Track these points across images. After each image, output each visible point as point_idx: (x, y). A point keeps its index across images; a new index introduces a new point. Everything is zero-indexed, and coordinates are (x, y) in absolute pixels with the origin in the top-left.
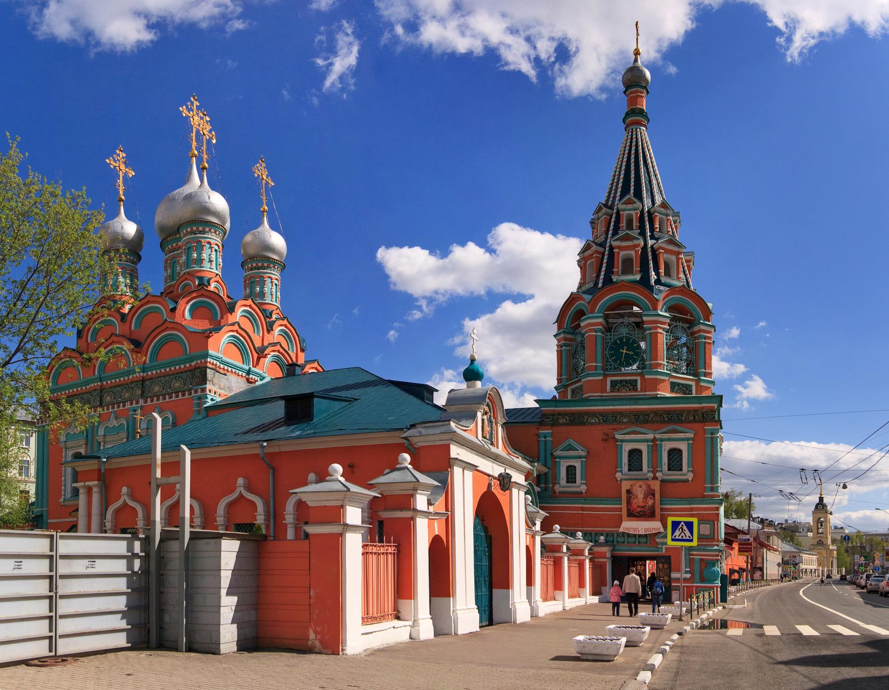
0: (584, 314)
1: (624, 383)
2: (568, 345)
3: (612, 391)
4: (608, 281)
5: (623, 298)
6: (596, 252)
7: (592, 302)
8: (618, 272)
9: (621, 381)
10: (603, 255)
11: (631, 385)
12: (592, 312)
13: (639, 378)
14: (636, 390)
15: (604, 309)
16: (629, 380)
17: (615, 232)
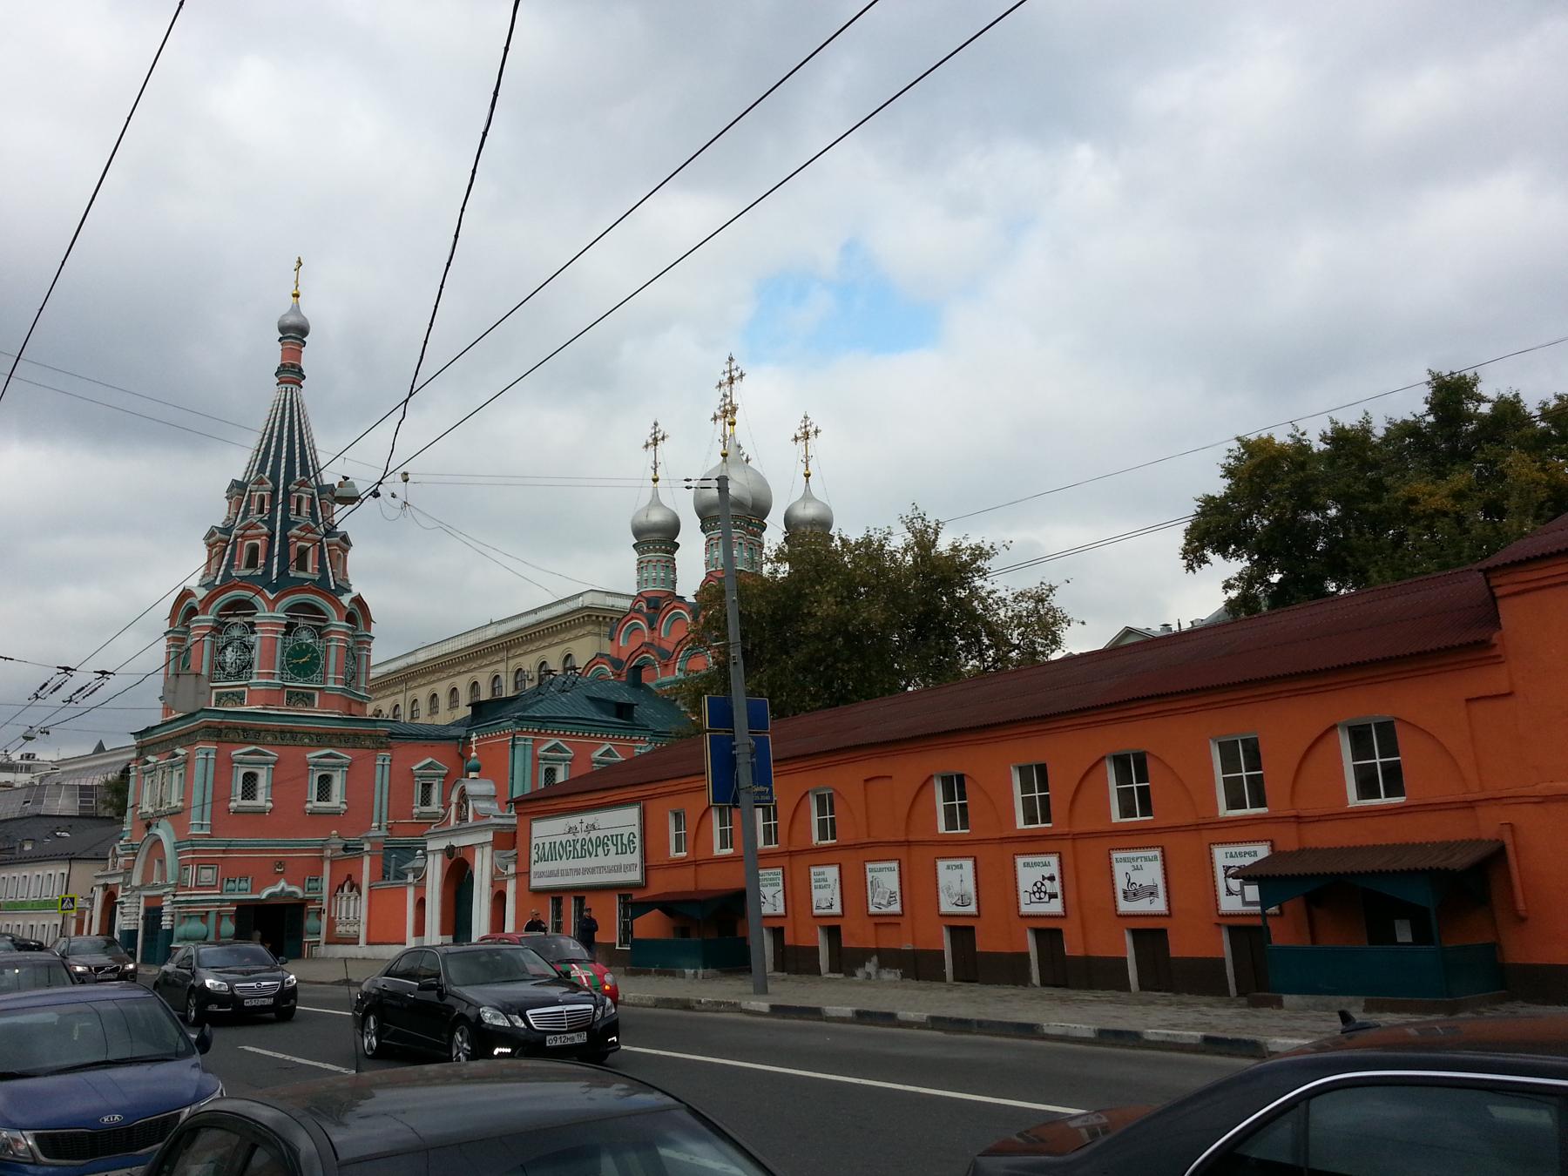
0: (197, 614)
1: (230, 696)
2: (178, 647)
3: (216, 706)
4: (227, 575)
5: (238, 598)
6: (221, 541)
7: (204, 601)
8: (239, 566)
9: (227, 694)
10: (227, 542)
11: (238, 698)
12: (205, 611)
13: (246, 689)
14: (242, 705)
15: (219, 607)
16: (237, 692)
17: (244, 517)
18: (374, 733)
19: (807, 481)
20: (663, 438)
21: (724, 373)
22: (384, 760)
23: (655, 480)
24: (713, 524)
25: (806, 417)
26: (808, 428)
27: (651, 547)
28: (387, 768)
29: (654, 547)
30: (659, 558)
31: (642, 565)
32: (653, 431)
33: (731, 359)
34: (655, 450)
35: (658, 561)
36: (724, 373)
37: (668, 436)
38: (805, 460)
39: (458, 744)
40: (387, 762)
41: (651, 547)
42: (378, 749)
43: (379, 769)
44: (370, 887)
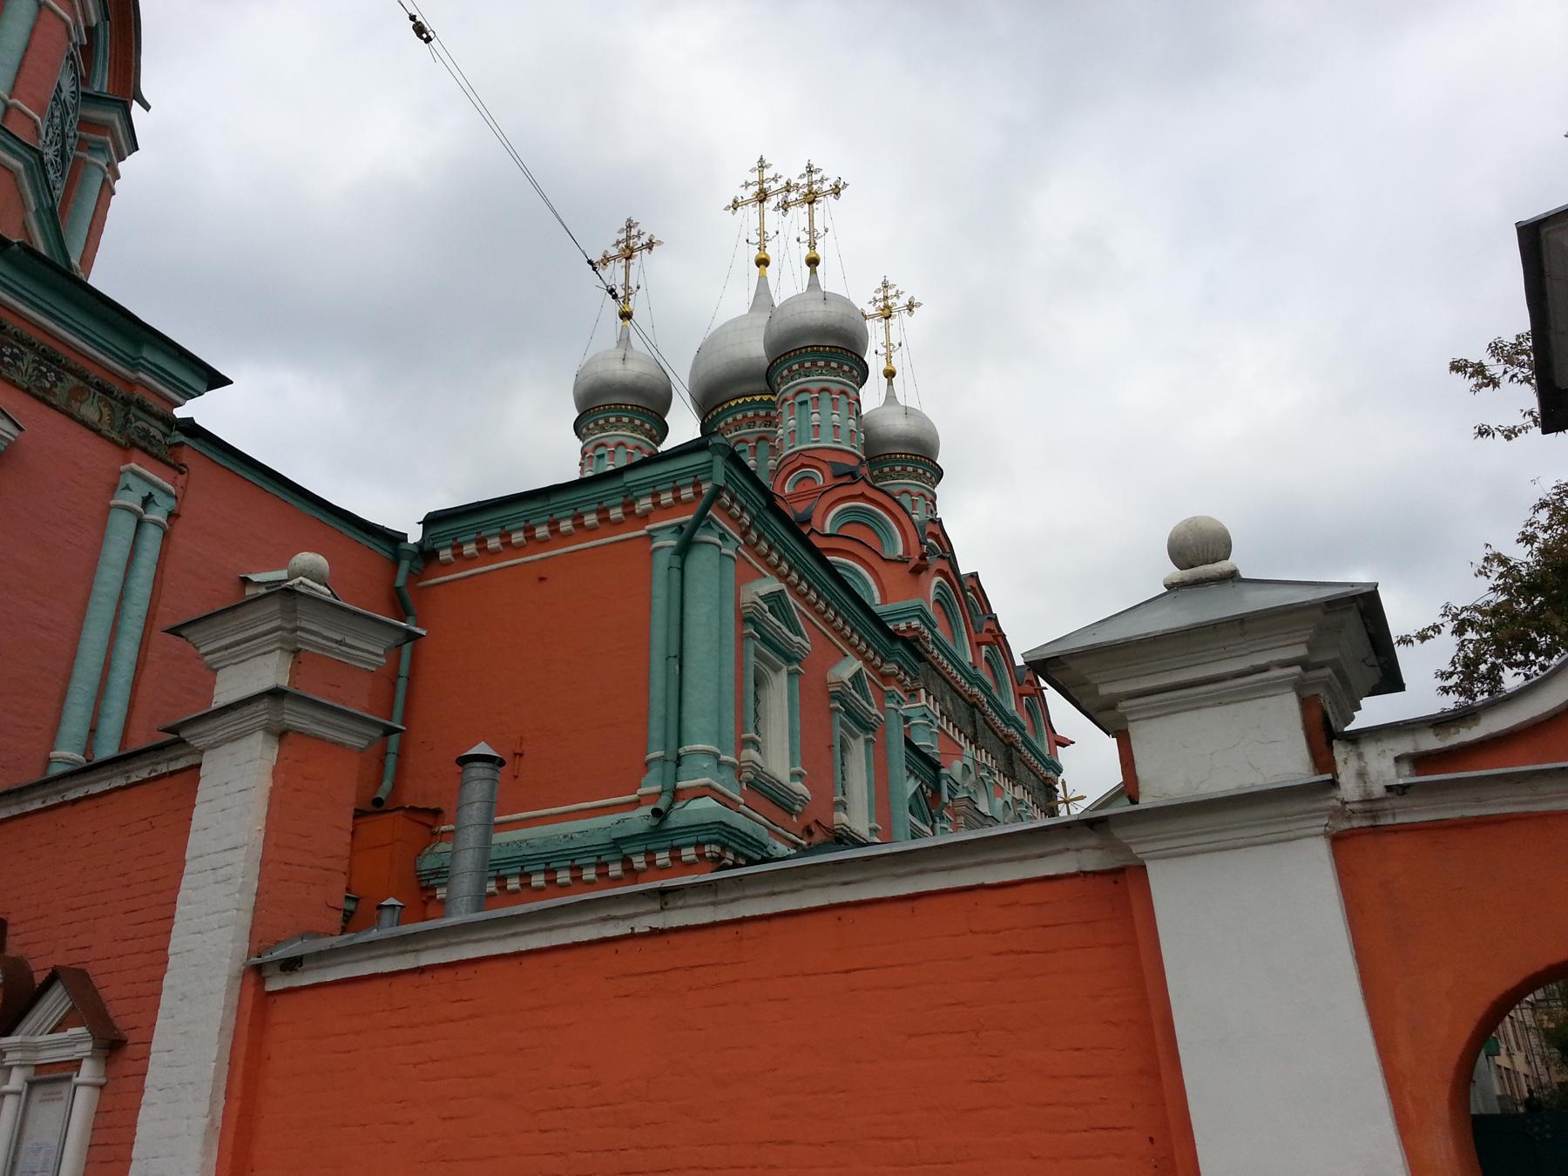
18: (117, 387)
19: (890, 383)
20: (650, 246)
21: (747, 185)
22: (147, 501)
23: (626, 316)
24: (808, 365)
25: (886, 286)
26: (890, 302)
27: (625, 420)
28: (152, 541)
29: (631, 421)
30: (639, 443)
31: (600, 451)
32: (624, 236)
33: (762, 165)
34: (627, 268)
35: (638, 448)
36: (747, 185)
37: (660, 243)
38: (882, 350)
39: (396, 564)
40: (157, 514)
41: (625, 420)
42: (128, 447)
43: (121, 527)
44: (256, 972)
